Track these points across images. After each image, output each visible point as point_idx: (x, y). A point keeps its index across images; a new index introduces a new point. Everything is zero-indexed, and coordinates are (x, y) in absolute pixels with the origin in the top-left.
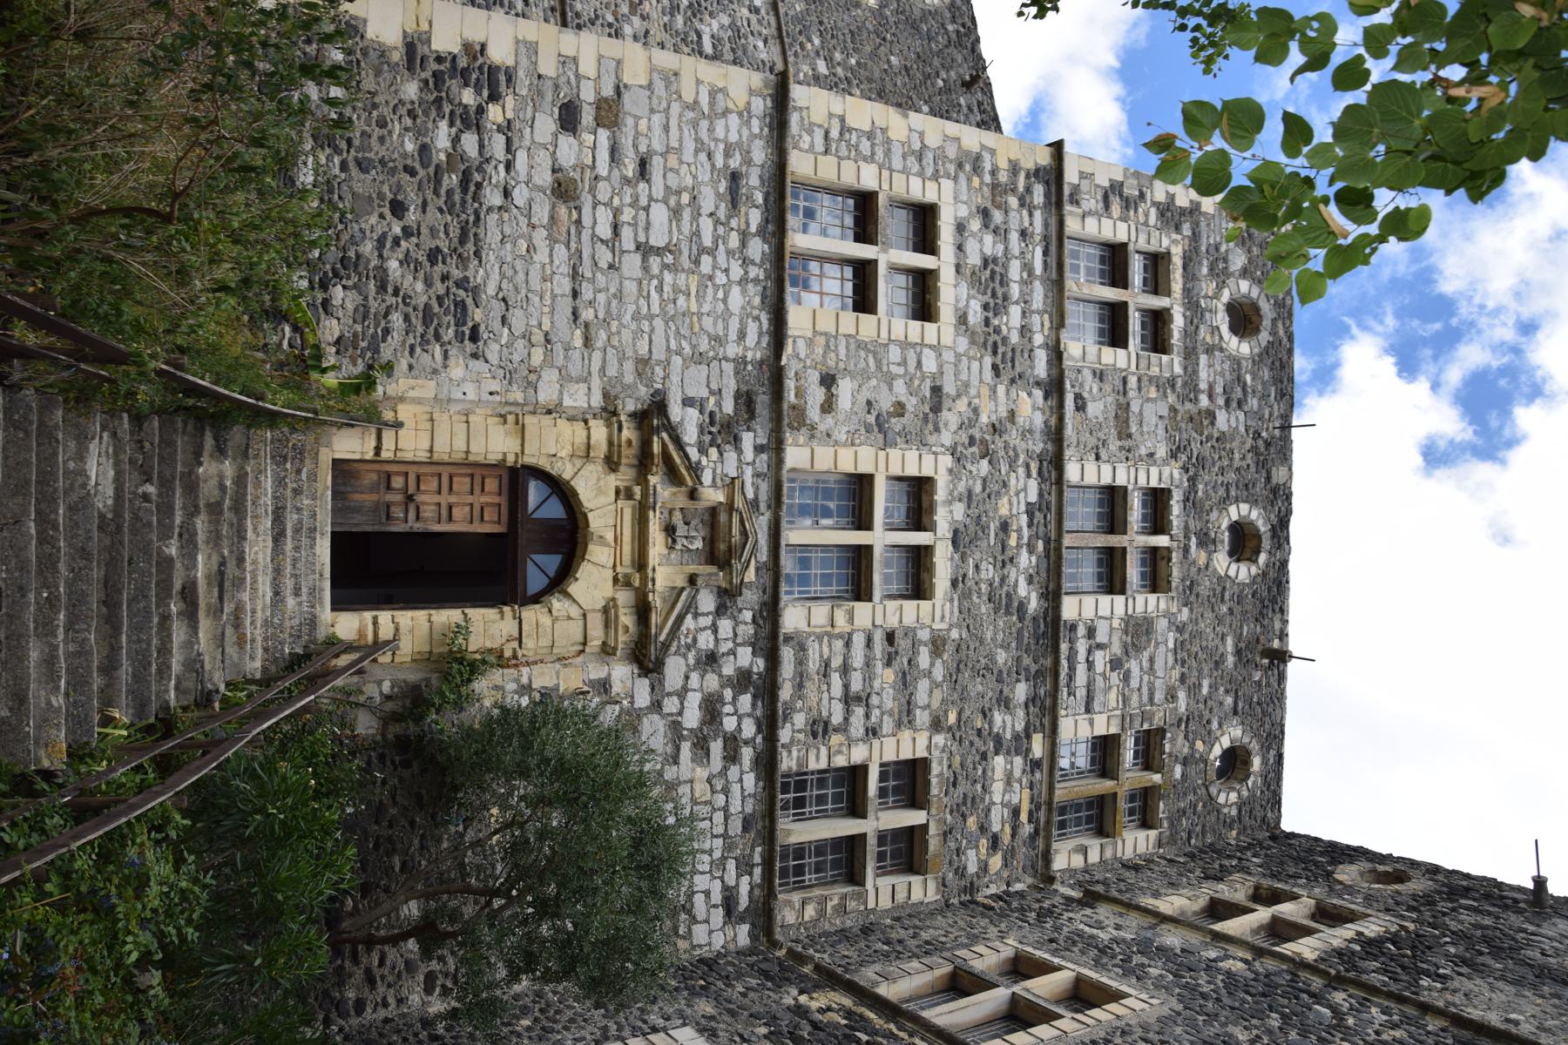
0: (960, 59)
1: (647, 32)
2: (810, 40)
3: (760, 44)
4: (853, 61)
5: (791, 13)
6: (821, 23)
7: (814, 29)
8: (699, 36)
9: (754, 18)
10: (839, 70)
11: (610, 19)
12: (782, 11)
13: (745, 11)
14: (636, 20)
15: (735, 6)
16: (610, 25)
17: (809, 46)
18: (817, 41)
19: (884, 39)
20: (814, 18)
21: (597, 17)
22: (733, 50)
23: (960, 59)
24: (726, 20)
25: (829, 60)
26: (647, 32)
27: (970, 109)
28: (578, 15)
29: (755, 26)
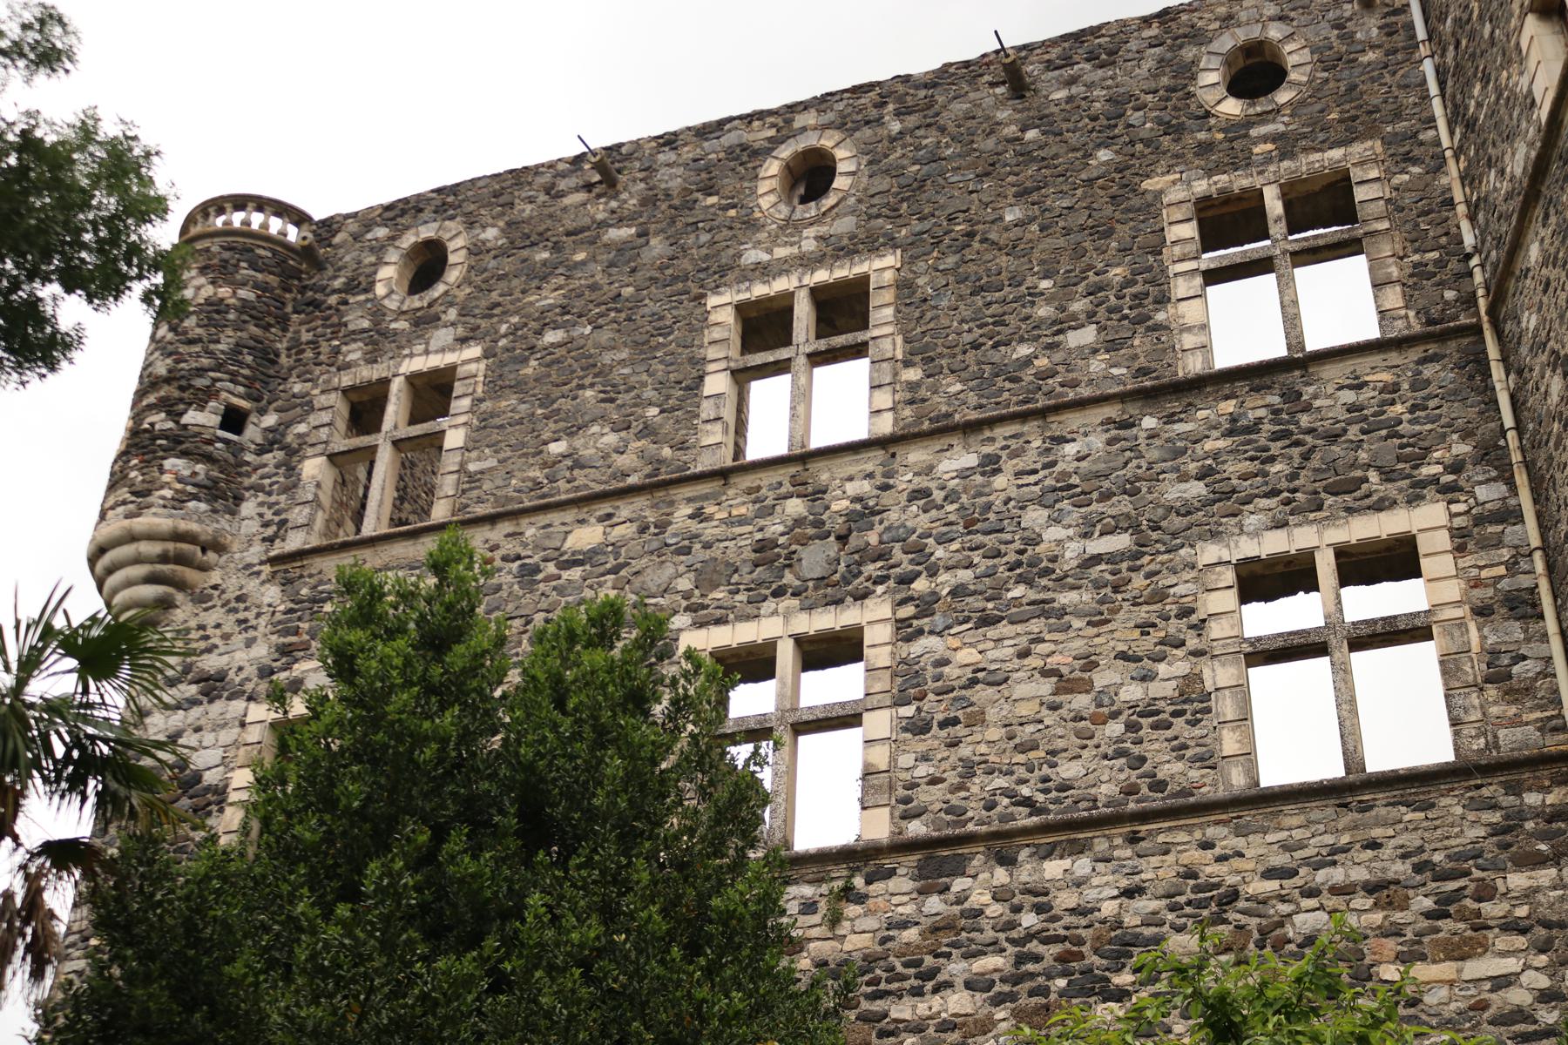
0: (959, 107)
1: (1123, 656)
2: (1028, 362)
3: (1070, 449)
4: (1045, 284)
5: (972, 399)
6: (976, 346)
7: (996, 356)
8: (1096, 559)
9: (1009, 466)
10: (1078, 306)
11: (1116, 728)
12: (974, 415)
13: (1000, 481)
14: (1100, 679)
15: (997, 501)
16: (1132, 727)
17: (1042, 362)
18: (1024, 350)
19: (971, 235)
20: (971, 356)
21: (1121, 753)
22: (1106, 496)
23: (959, 107)
24: (1035, 517)
25: (1063, 324)
26: (1123, 656)
27: (1072, 81)
28: (1130, 790)
29: (1030, 459)
